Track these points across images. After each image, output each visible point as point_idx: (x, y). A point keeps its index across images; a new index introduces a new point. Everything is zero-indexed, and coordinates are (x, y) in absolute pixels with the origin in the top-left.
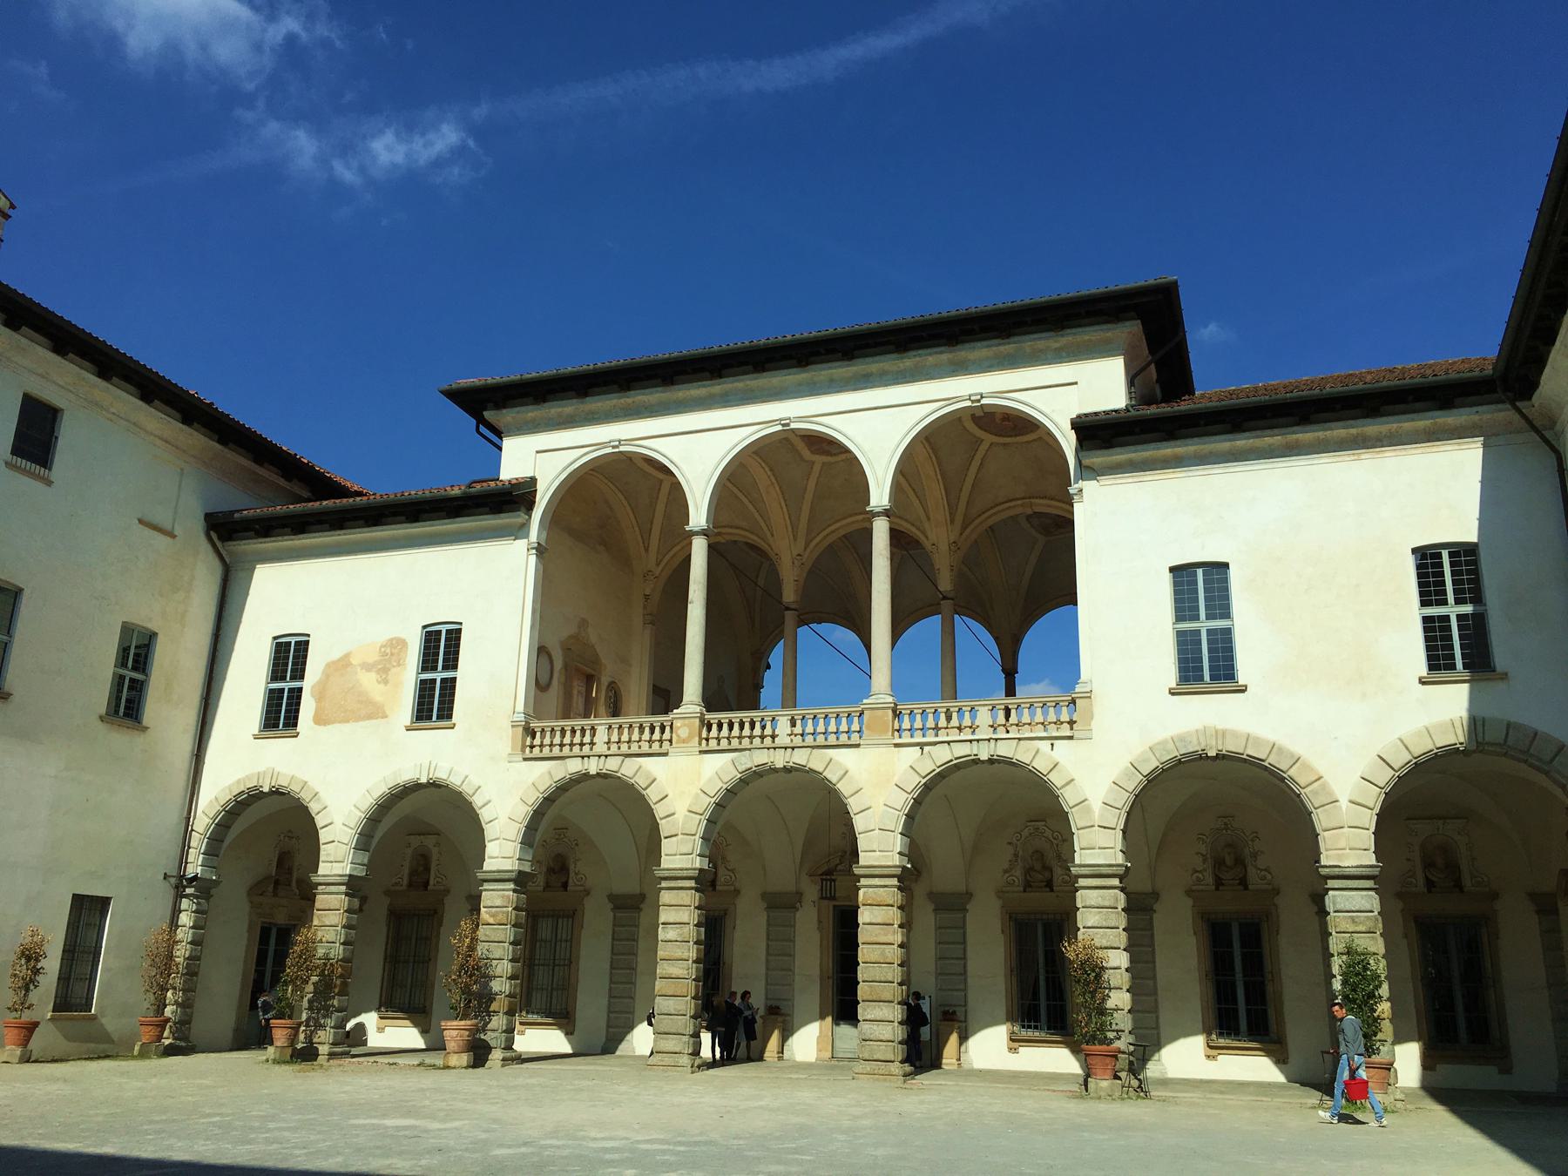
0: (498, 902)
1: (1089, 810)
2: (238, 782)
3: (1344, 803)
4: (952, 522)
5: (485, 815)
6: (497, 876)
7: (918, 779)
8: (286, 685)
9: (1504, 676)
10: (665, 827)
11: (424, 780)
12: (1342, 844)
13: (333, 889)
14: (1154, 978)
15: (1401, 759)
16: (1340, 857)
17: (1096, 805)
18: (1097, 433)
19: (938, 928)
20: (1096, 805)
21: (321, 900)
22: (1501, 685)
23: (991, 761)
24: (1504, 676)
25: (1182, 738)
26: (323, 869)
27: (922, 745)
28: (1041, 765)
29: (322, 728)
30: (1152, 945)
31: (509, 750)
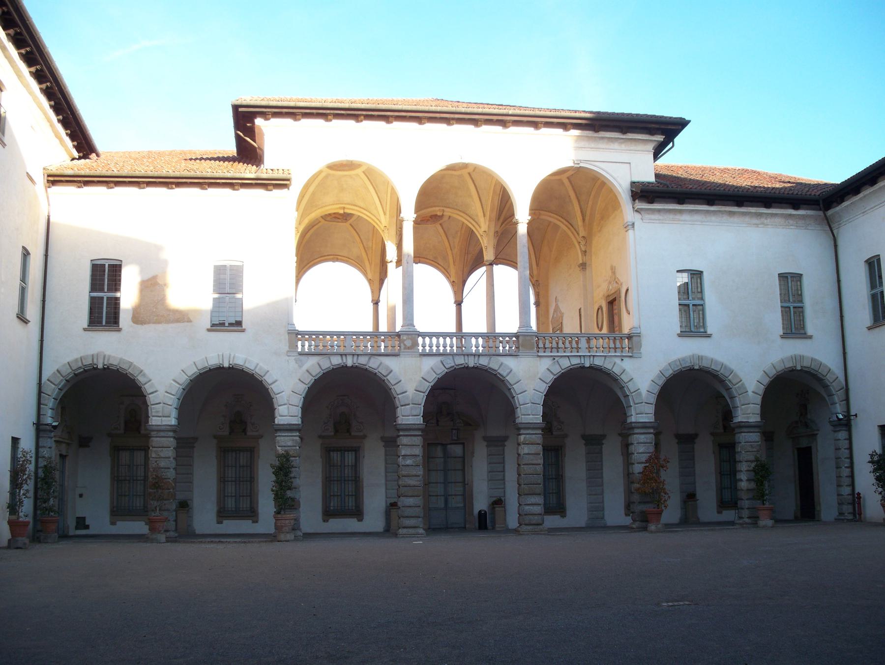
0: (290, 444)
1: (640, 394)
2: (76, 360)
3: (750, 393)
4: (499, 219)
5: (274, 388)
6: (288, 427)
7: (552, 376)
8: (105, 295)
9: (810, 337)
10: (400, 399)
11: (226, 365)
12: (749, 412)
13: (162, 434)
14: (602, 477)
15: (773, 373)
16: (748, 418)
17: (644, 392)
18: (643, 194)
19: (489, 455)
20: (644, 392)
21: (155, 441)
22: (808, 342)
23: (590, 367)
24: (810, 337)
25: (684, 359)
26: (154, 421)
27: (554, 358)
28: (616, 370)
29: (139, 326)
30: (601, 461)
31: (287, 348)
